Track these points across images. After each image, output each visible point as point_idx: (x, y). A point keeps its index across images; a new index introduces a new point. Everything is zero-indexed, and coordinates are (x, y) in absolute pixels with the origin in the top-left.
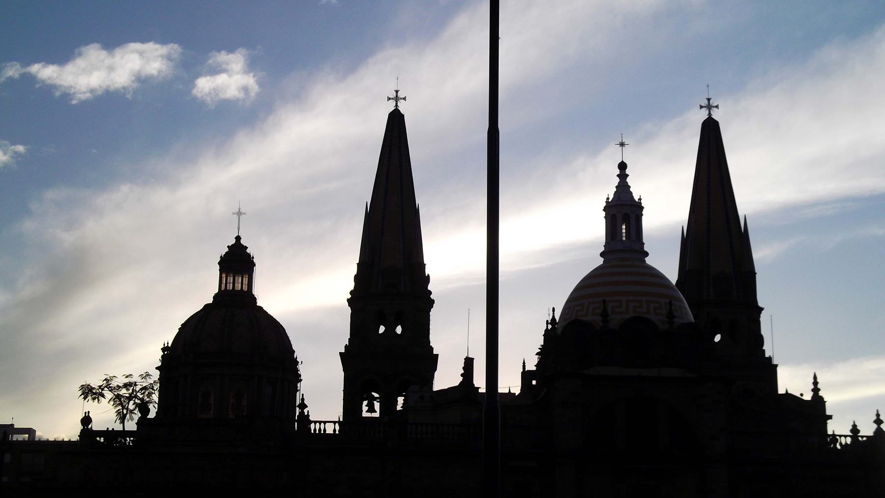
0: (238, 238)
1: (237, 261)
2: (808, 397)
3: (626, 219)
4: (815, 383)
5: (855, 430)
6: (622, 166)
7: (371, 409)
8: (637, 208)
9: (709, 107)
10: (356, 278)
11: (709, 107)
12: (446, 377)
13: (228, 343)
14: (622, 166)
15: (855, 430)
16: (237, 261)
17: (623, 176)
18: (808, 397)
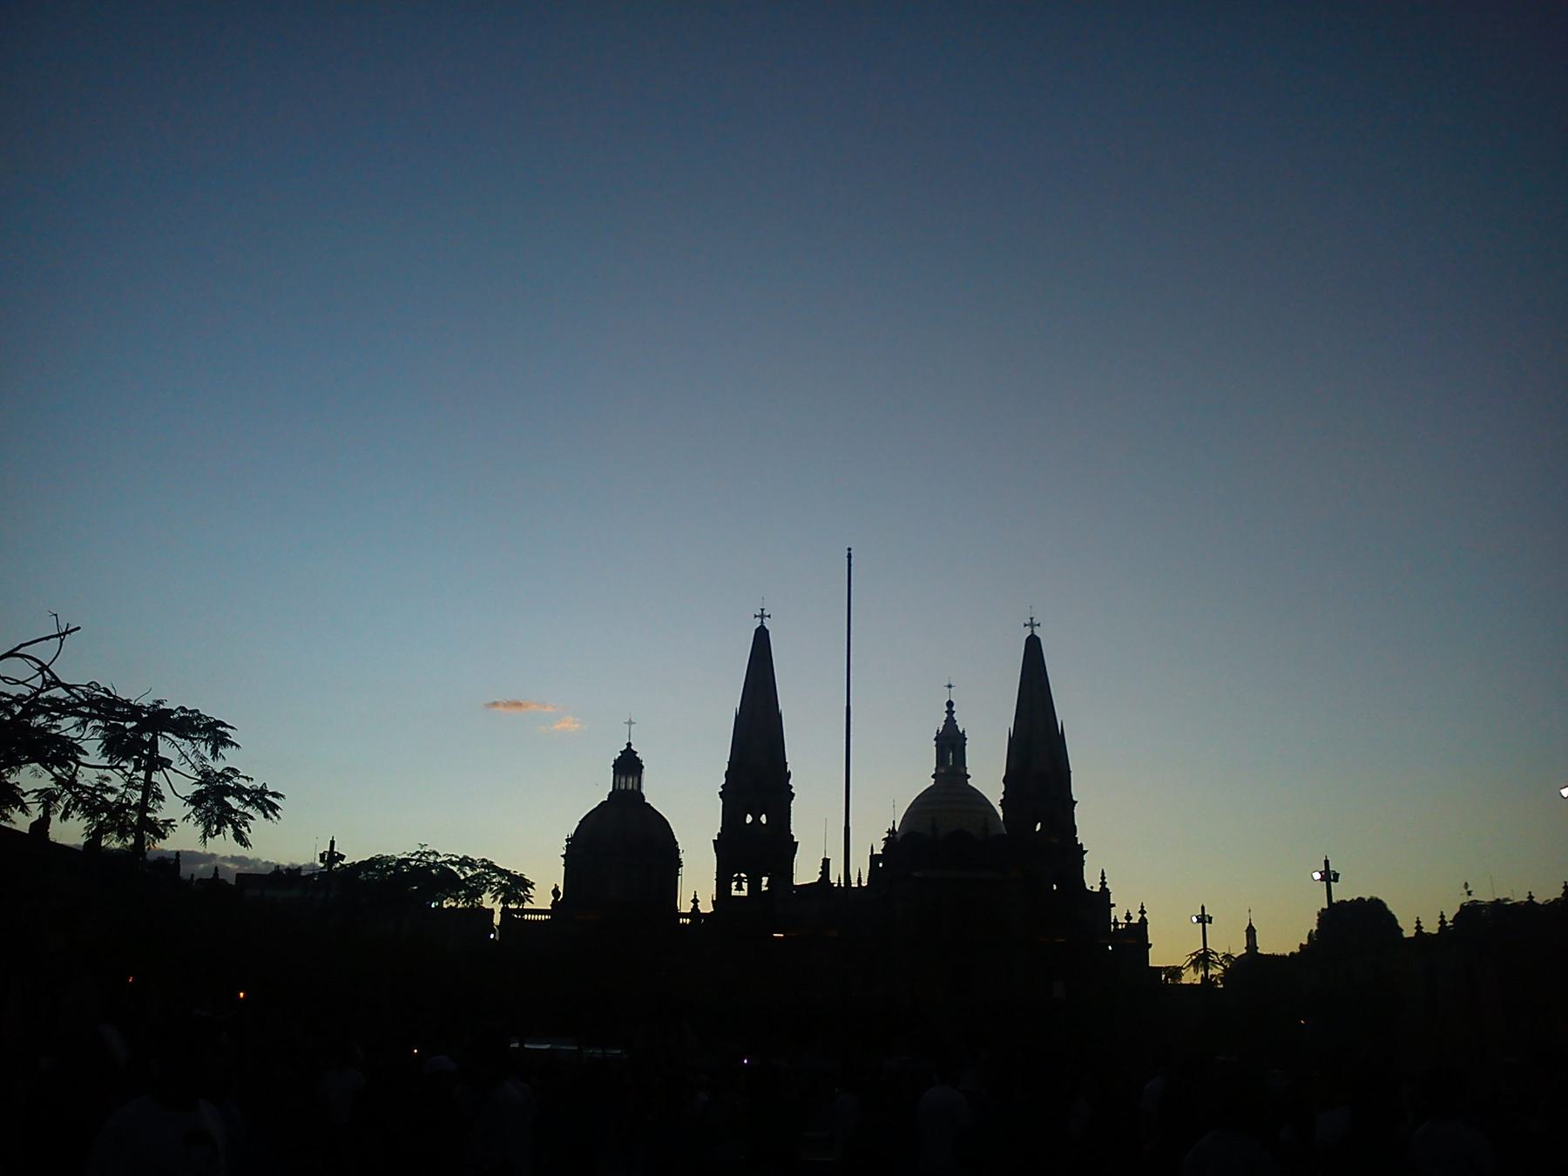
0: (629, 744)
1: (628, 764)
2: (1097, 889)
3: (953, 748)
4: (1103, 878)
5: (1128, 917)
6: (950, 704)
7: (739, 888)
8: (962, 738)
9: (1032, 625)
10: (727, 774)
11: (1032, 625)
12: (805, 872)
13: (621, 838)
14: (950, 704)
15: (1128, 917)
16: (628, 764)
17: (950, 712)
18: (1097, 889)
